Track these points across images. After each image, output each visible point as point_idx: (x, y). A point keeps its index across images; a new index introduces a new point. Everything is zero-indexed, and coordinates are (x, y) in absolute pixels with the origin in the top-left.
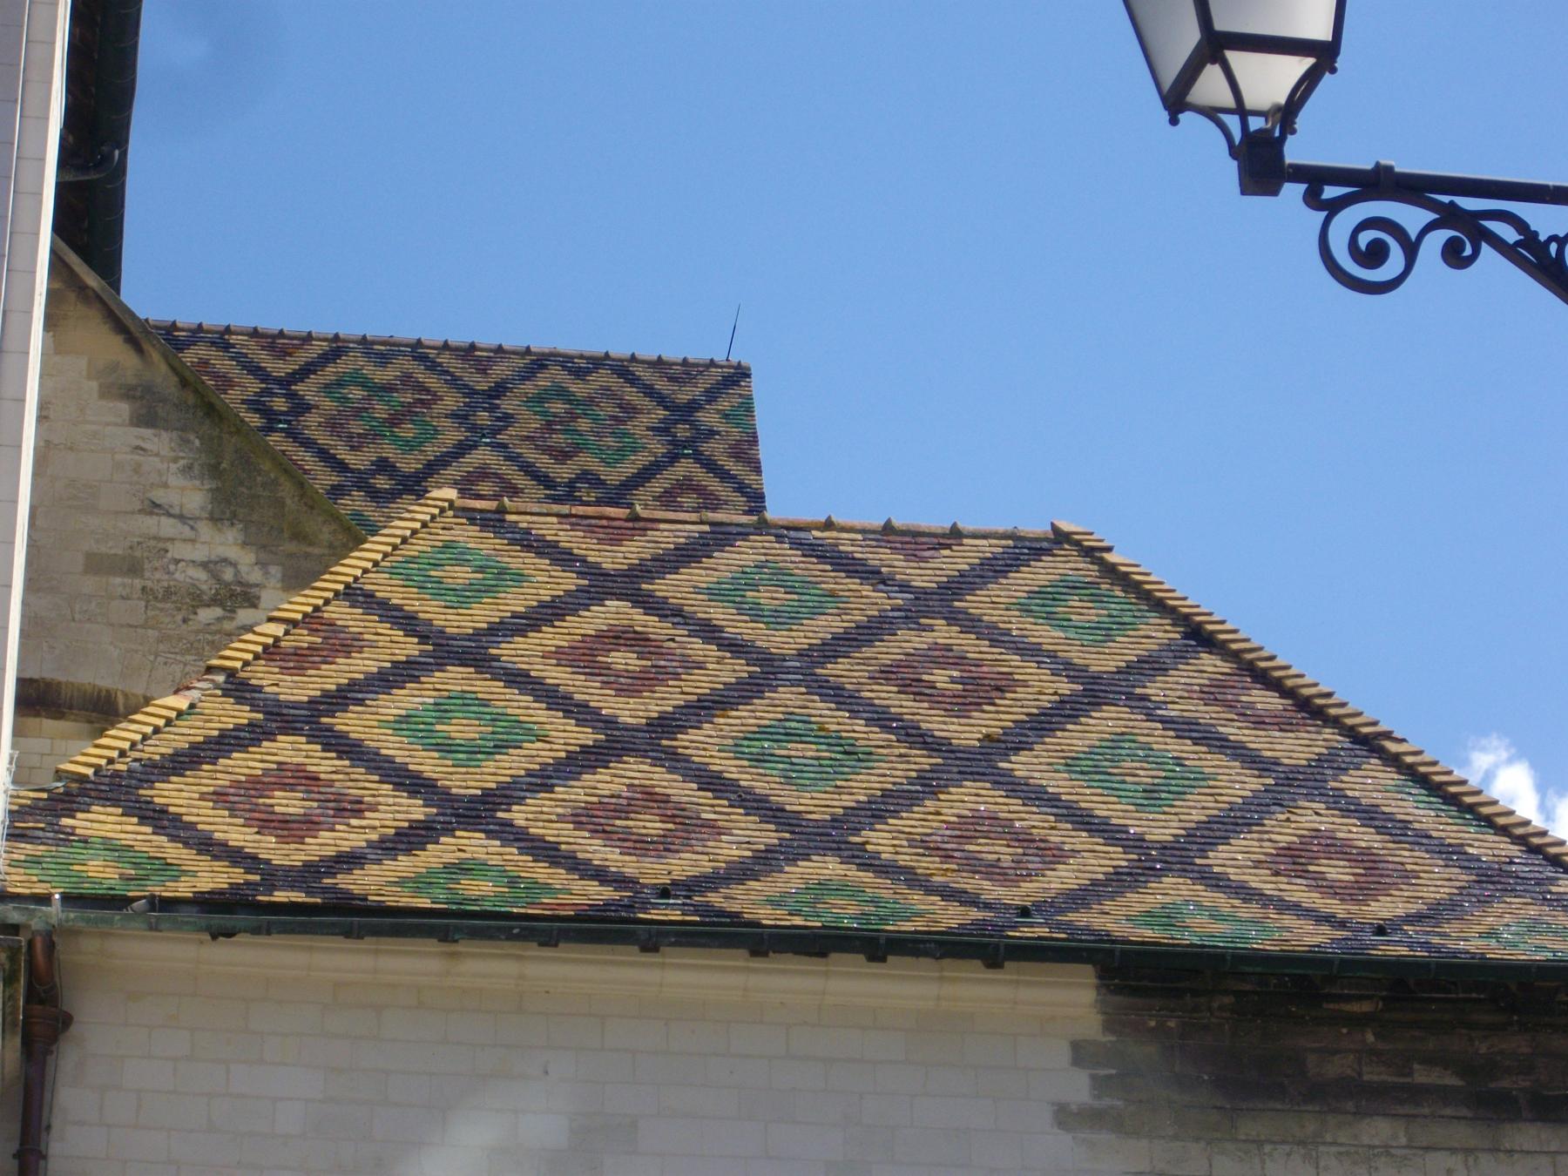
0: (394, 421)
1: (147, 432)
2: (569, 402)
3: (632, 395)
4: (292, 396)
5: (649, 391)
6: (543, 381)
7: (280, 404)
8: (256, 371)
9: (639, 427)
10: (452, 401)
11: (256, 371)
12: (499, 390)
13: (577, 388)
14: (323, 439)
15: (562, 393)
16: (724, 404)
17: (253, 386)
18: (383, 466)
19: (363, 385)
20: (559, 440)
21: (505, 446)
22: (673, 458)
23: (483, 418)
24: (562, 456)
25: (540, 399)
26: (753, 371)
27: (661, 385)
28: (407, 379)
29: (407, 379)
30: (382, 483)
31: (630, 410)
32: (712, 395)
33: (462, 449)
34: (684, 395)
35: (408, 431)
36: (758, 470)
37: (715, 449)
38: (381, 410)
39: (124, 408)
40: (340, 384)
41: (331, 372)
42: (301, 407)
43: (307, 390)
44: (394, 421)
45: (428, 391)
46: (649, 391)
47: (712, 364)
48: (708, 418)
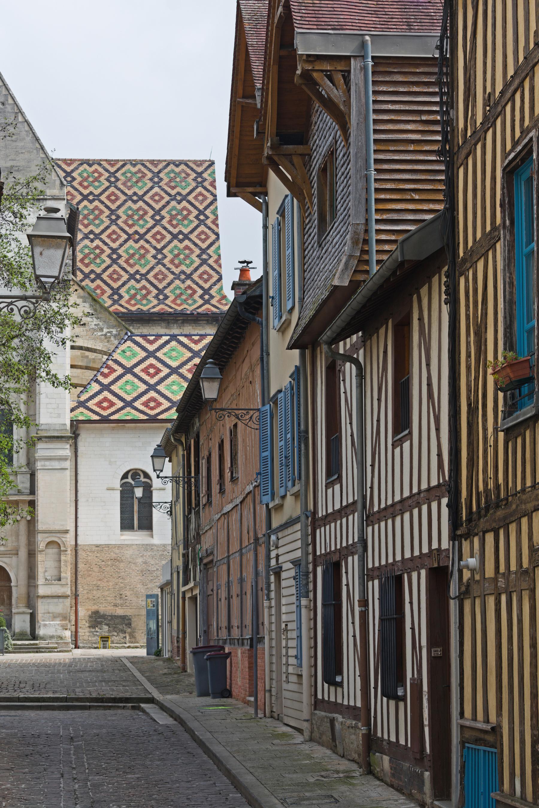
0: (137, 182)
1: (85, 304)
2: (175, 174)
3: (189, 171)
4: (115, 177)
5: (192, 169)
6: (169, 168)
7: (113, 179)
8: (107, 170)
9: (190, 179)
10: (150, 175)
11: (107, 170)
12: (160, 172)
13: (177, 170)
14: (122, 187)
15: (173, 171)
16: (209, 171)
17: (107, 175)
18: (135, 194)
19: (130, 173)
20: (173, 184)
21: (161, 186)
22: (197, 187)
23: (156, 180)
24: (173, 188)
25: (169, 173)
26: (215, 162)
27: (195, 167)
28: (140, 171)
29: (140, 171)
30: (135, 198)
31: (188, 175)
32: (206, 169)
33: (152, 188)
34: (200, 170)
35: (140, 184)
36: (215, 189)
37: (206, 184)
38: (134, 180)
39: (81, 300)
40: (125, 173)
41: (123, 170)
42: (117, 180)
43: (118, 175)
44: (137, 182)
45: (144, 173)
46: (192, 169)
47: (206, 161)
48: (205, 175)
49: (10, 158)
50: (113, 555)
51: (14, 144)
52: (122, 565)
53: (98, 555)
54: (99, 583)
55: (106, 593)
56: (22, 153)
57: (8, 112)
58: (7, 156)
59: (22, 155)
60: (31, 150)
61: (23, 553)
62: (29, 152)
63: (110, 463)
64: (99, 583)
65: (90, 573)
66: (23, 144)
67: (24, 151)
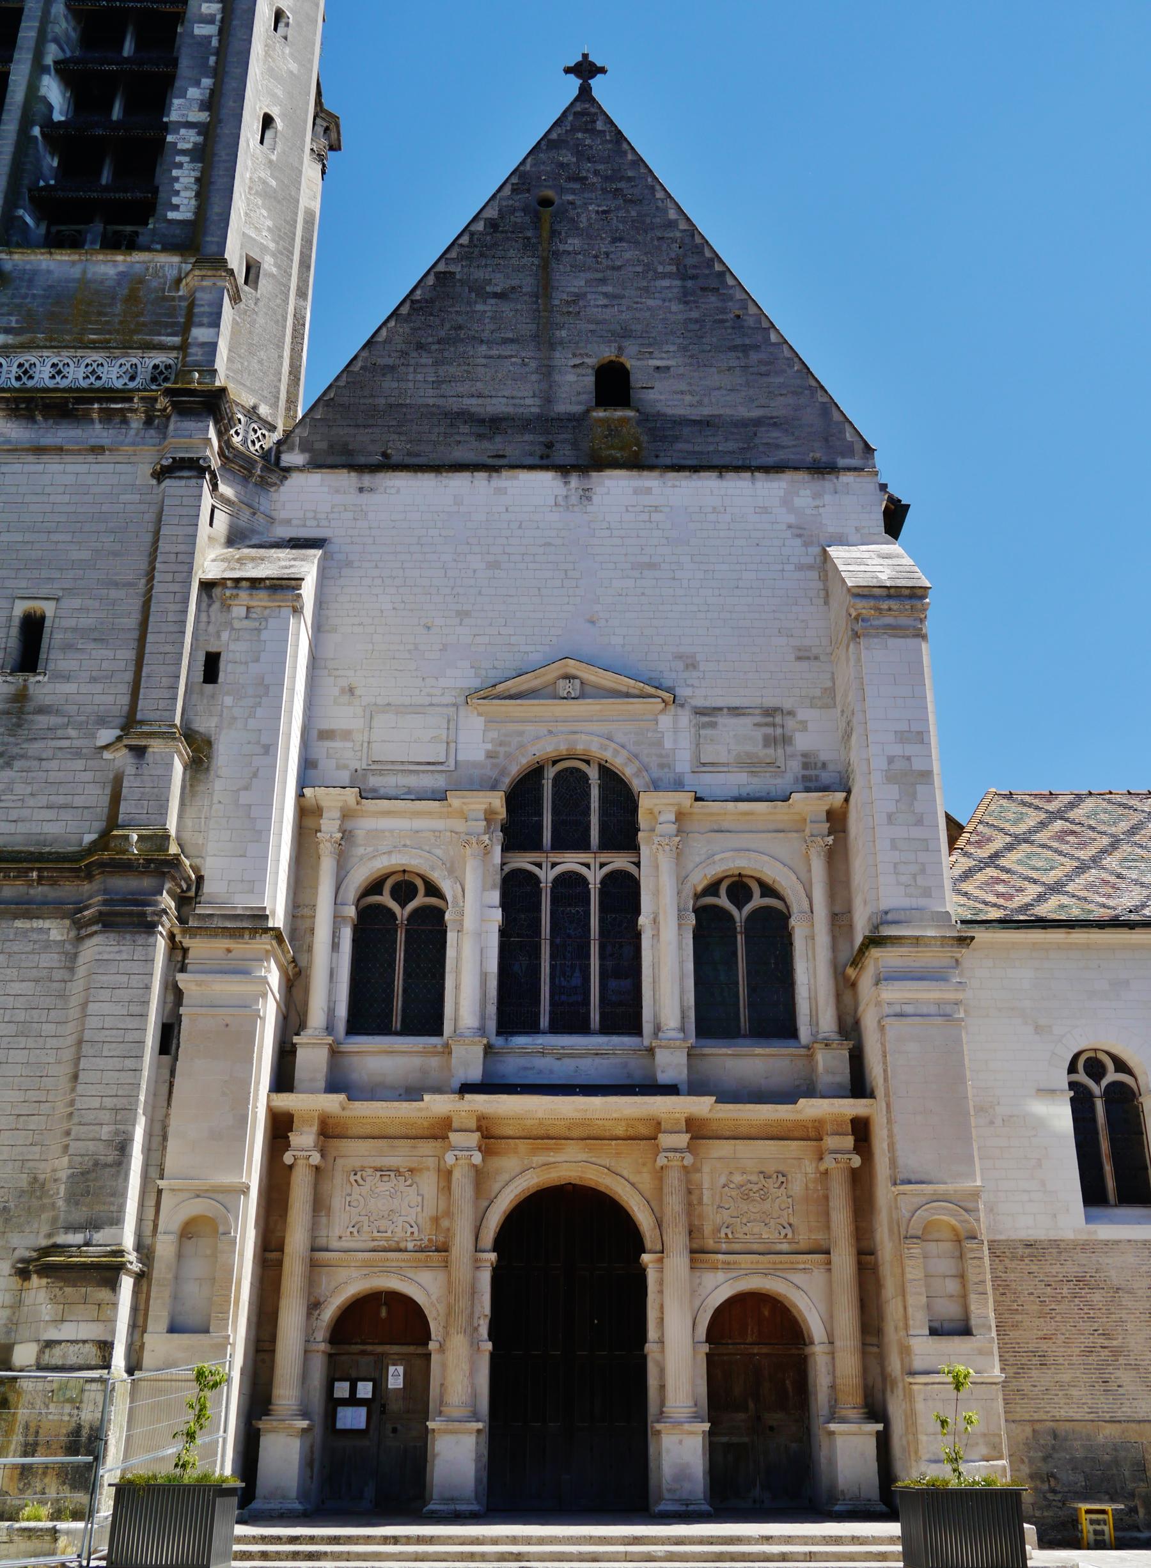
49: (756, 403)
50: (1071, 1269)
51: (765, 379)
52: (1097, 1297)
53: (1034, 1268)
54: (1044, 1345)
55: (1066, 1377)
56: (781, 395)
57: (749, 328)
58: (752, 400)
59: (782, 398)
60: (800, 390)
61: (844, 1259)
62: (794, 393)
63: (1038, 1030)
64: (1044, 1345)
65: (1018, 1317)
66: (782, 380)
67: (785, 392)
